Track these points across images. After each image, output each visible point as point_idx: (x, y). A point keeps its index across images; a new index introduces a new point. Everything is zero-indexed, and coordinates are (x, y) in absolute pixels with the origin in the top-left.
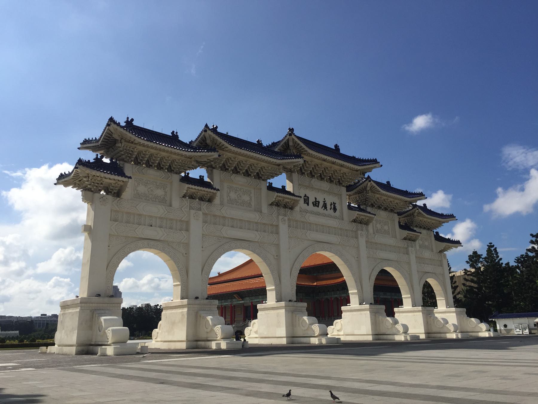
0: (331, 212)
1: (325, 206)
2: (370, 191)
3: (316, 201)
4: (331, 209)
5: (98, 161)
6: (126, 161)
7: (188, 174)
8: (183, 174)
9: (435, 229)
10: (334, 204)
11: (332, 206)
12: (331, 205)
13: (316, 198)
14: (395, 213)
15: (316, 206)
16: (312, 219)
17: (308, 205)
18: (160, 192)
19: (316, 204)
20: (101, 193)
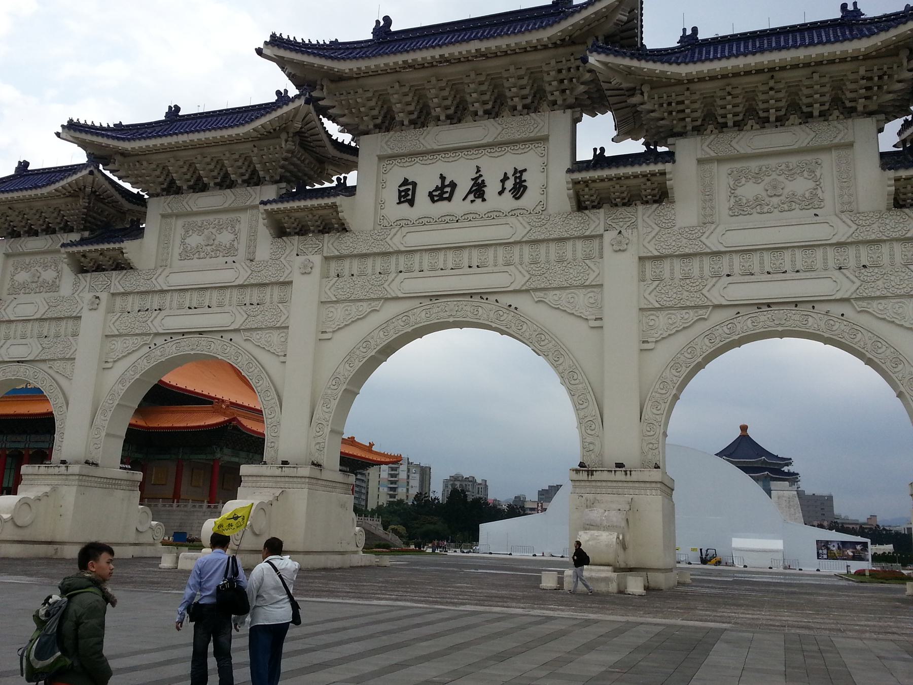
1: (478, 190)
2: (646, 89)
3: (443, 186)
4: (500, 193)
10: (519, 174)
11: (509, 184)
12: (506, 178)
13: (443, 178)
15: (441, 199)
16: (416, 239)
17: (411, 203)
18: (49, 275)
19: (443, 192)
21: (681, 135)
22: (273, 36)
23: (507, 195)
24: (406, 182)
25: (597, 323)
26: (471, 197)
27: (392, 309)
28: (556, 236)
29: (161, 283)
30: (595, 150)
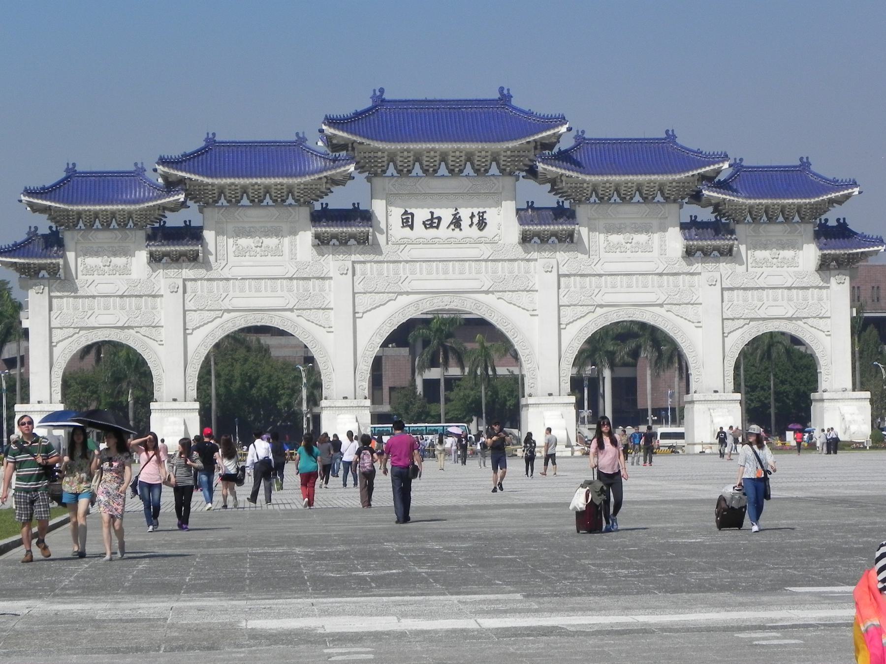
0: (469, 231)
1: (457, 222)
4: (471, 226)
5: (33, 234)
6: (68, 228)
7: (165, 222)
8: (157, 225)
9: (820, 215)
10: (481, 215)
11: (476, 220)
12: (473, 216)
13: (432, 213)
14: (675, 201)
15: (431, 226)
19: (433, 223)
20: (41, 275)
21: (580, 202)
22: (326, 118)
23: (475, 227)
24: (406, 213)
25: (534, 313)
26: (452, 226)
27: (403, 300)
28: (508, 258)
29: (226, 273)
30: (528, 202)
